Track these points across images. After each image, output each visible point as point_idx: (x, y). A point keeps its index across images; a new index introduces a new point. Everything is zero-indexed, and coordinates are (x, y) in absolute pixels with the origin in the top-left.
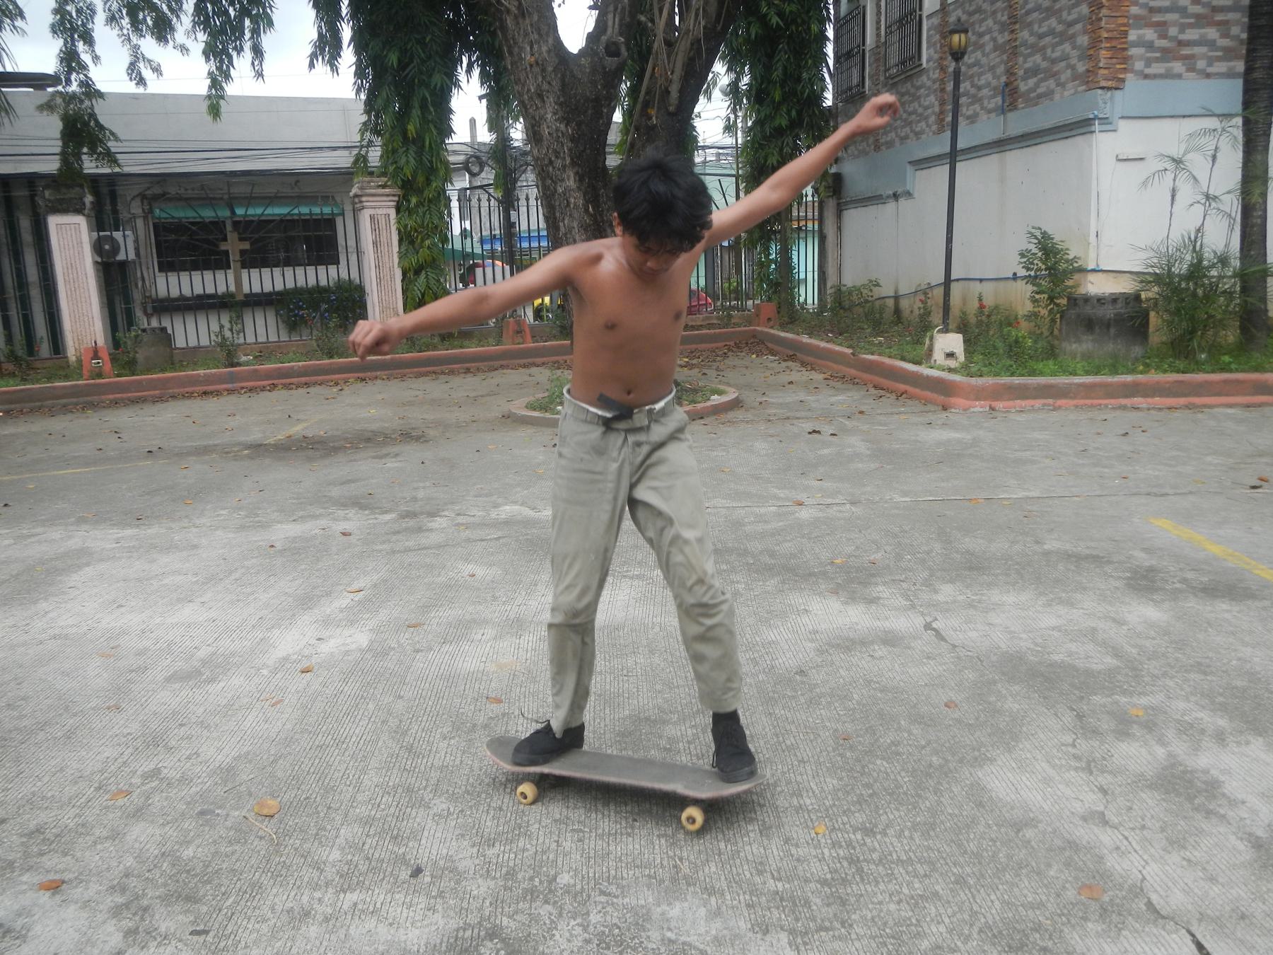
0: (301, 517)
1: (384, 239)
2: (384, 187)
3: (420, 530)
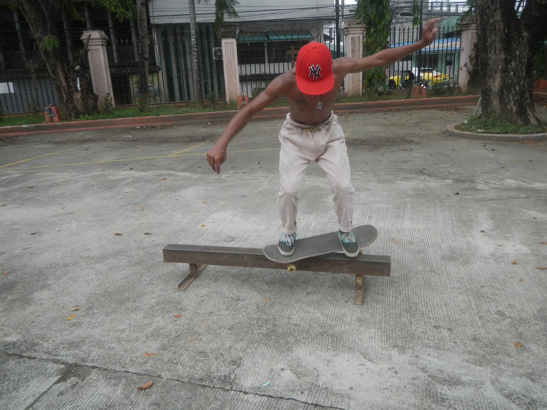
1: (356, 49)
2: (359, 24)
3: (475, 189)
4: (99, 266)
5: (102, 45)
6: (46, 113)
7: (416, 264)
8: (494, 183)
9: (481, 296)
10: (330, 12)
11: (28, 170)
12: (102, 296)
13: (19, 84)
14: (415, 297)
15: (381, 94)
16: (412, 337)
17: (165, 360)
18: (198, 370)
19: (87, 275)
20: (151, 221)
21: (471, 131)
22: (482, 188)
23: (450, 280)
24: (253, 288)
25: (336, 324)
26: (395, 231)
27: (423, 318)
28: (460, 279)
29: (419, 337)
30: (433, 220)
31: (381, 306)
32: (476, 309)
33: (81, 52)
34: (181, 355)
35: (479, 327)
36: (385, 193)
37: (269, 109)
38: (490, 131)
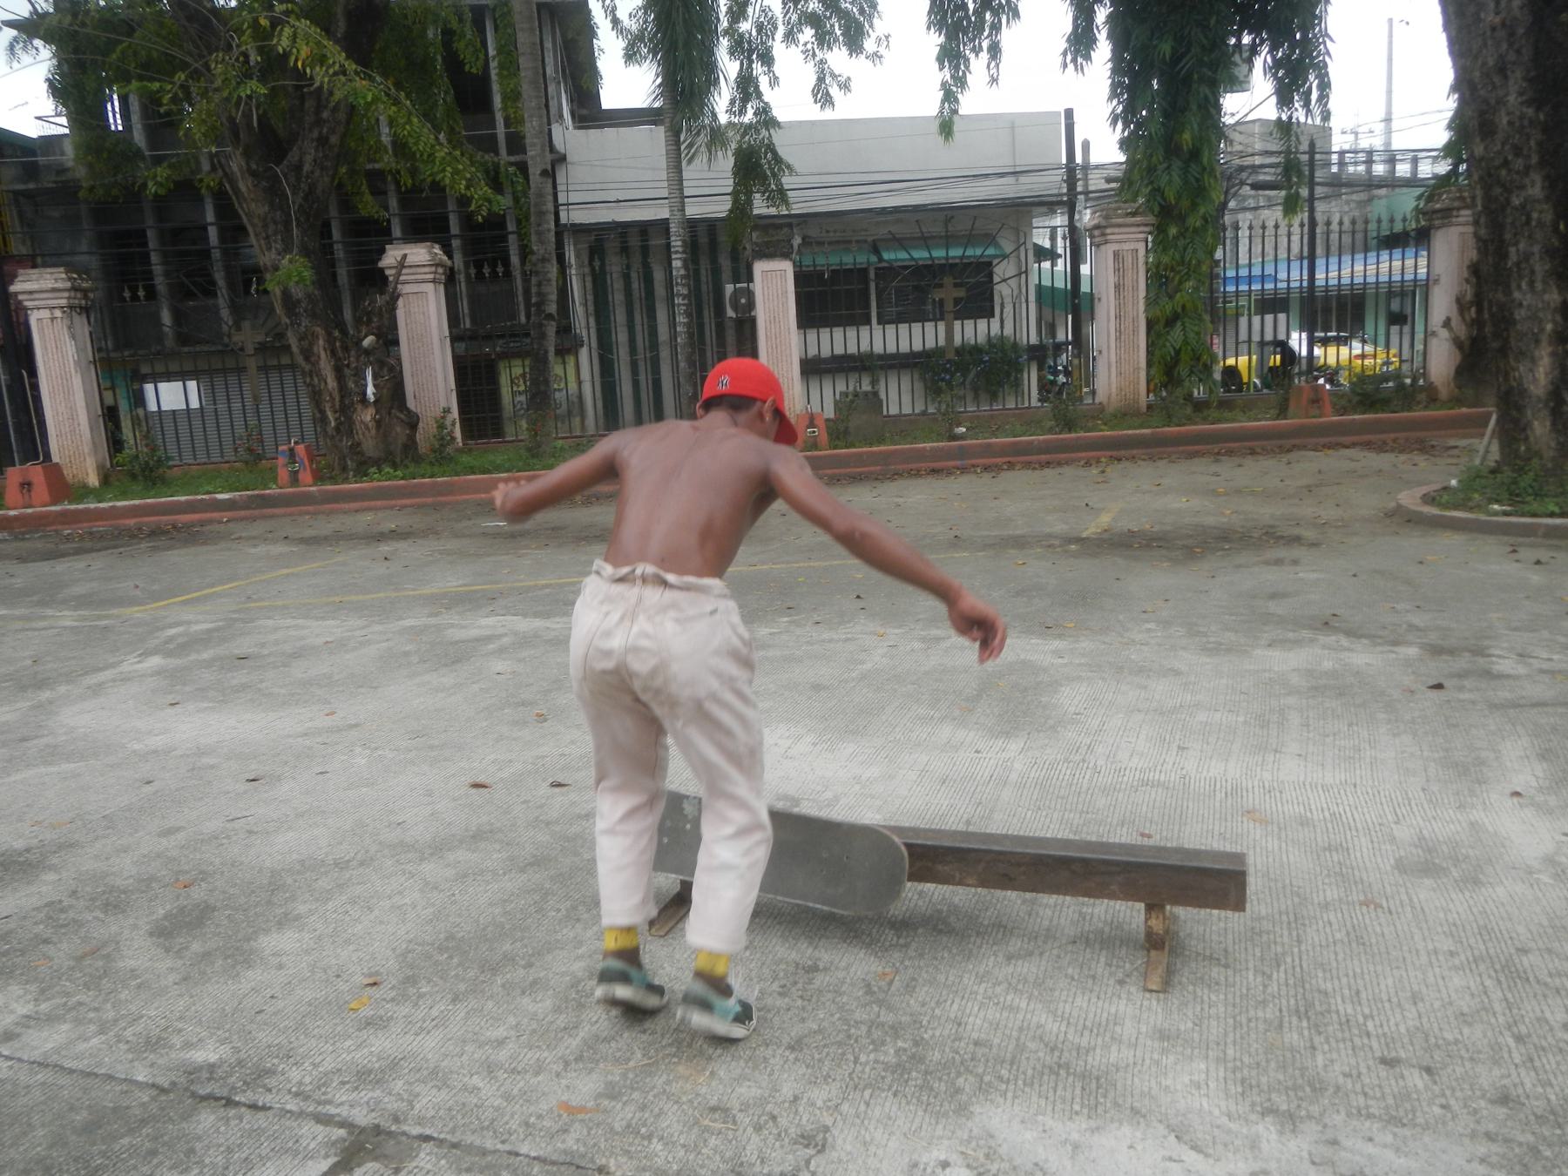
0: (1274, 641)
1: (1128, 282)
2: (1134, 214)
3: (1488, 674)
4: (429, 869)
5: (434, 281)
6: (282, 460)
7: (1320, 883)
8: (1545, 656)
9: (1520, 978)
10: (1053, 183)
11: (234, 612)
12: (441, 949)
13: (212, 382)
14: (1320, 975)
15: (1200, 406)
16: (1318, 1087)
17: (618, 1127)
18: (708, 1157)
19: (400, 893)
20: (567, 750)
21: (1471, 509)
22: (1512, 672)
23: (1426, 934)
24: (855, 937)
25: (1093, 1043)
26: (1256, 789)
27: (1347, 1035)
28: (1453, 928)
29: (1338, 1088)
30: (1368, 760)
31: (1222, 997)
32: (1504, 1015)
33: (380, 300)
34: (659, 1115)
35: (1516, 1066)
36: (1224, 681)
37: (882, 448)
38: (1527, 508)
